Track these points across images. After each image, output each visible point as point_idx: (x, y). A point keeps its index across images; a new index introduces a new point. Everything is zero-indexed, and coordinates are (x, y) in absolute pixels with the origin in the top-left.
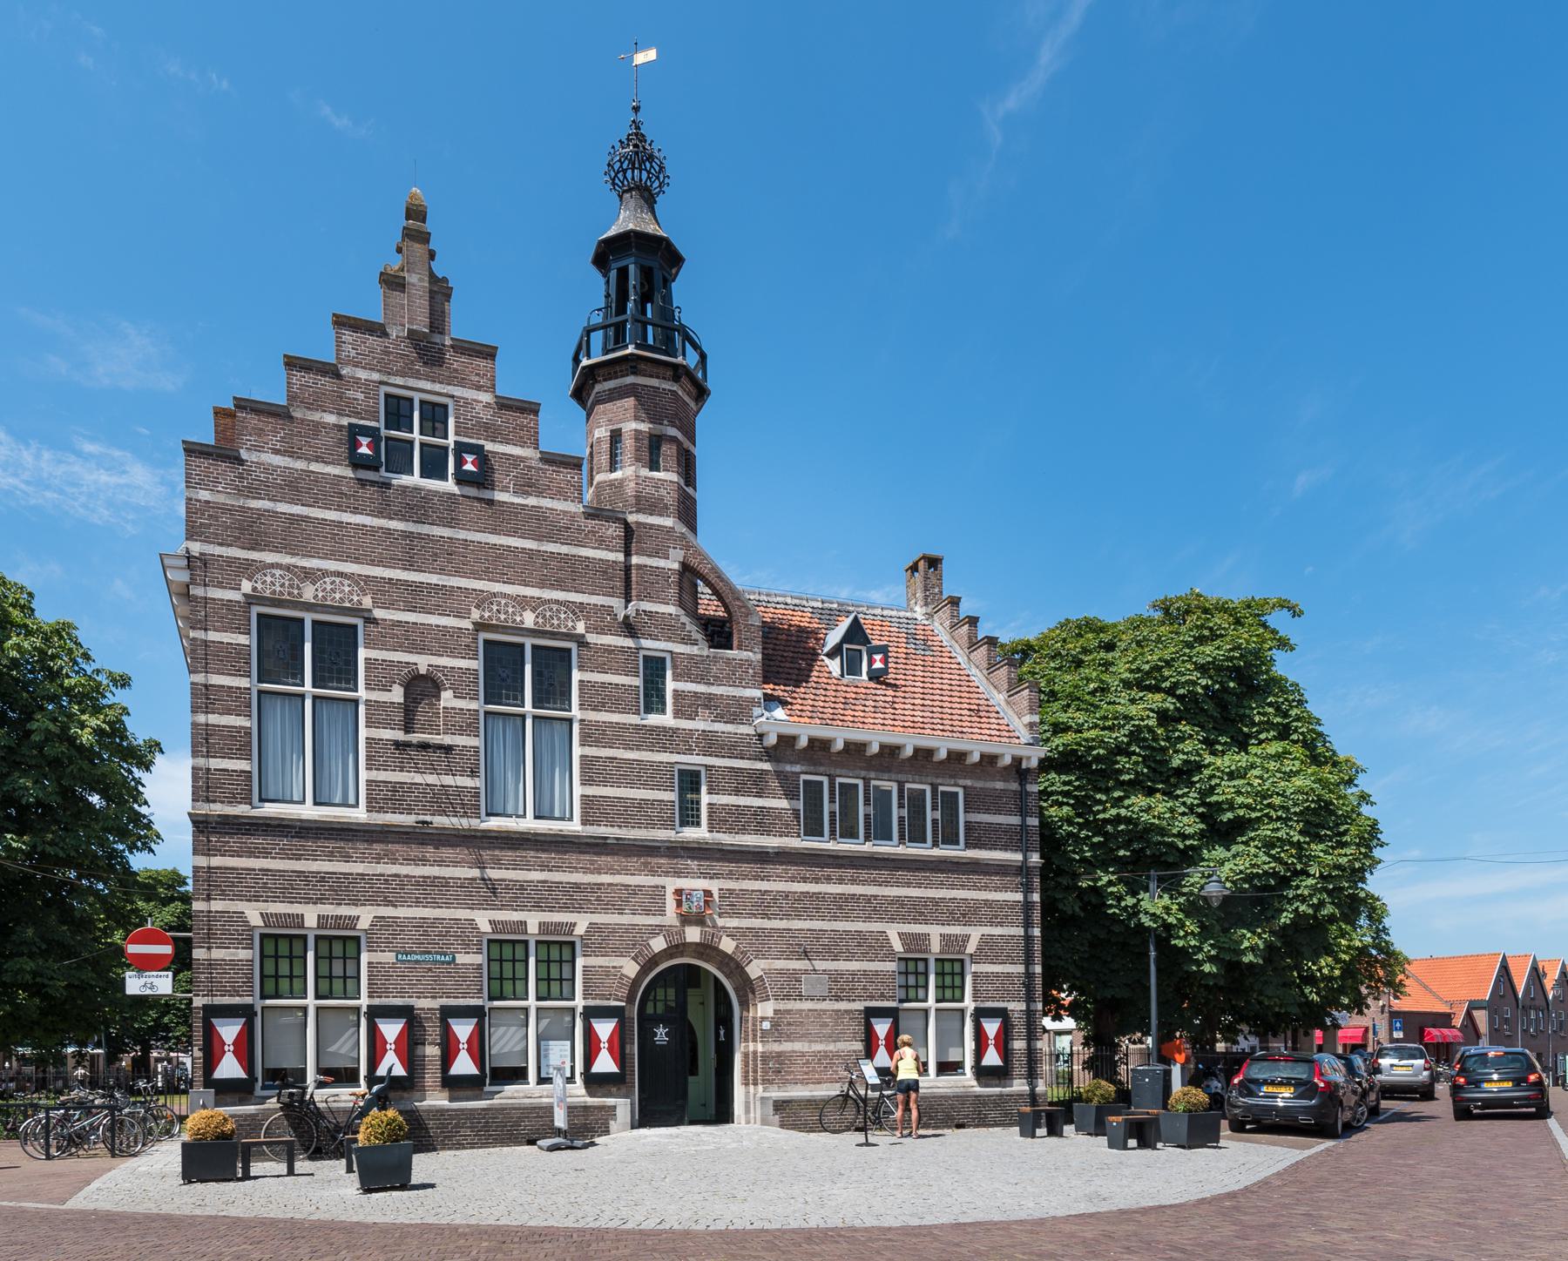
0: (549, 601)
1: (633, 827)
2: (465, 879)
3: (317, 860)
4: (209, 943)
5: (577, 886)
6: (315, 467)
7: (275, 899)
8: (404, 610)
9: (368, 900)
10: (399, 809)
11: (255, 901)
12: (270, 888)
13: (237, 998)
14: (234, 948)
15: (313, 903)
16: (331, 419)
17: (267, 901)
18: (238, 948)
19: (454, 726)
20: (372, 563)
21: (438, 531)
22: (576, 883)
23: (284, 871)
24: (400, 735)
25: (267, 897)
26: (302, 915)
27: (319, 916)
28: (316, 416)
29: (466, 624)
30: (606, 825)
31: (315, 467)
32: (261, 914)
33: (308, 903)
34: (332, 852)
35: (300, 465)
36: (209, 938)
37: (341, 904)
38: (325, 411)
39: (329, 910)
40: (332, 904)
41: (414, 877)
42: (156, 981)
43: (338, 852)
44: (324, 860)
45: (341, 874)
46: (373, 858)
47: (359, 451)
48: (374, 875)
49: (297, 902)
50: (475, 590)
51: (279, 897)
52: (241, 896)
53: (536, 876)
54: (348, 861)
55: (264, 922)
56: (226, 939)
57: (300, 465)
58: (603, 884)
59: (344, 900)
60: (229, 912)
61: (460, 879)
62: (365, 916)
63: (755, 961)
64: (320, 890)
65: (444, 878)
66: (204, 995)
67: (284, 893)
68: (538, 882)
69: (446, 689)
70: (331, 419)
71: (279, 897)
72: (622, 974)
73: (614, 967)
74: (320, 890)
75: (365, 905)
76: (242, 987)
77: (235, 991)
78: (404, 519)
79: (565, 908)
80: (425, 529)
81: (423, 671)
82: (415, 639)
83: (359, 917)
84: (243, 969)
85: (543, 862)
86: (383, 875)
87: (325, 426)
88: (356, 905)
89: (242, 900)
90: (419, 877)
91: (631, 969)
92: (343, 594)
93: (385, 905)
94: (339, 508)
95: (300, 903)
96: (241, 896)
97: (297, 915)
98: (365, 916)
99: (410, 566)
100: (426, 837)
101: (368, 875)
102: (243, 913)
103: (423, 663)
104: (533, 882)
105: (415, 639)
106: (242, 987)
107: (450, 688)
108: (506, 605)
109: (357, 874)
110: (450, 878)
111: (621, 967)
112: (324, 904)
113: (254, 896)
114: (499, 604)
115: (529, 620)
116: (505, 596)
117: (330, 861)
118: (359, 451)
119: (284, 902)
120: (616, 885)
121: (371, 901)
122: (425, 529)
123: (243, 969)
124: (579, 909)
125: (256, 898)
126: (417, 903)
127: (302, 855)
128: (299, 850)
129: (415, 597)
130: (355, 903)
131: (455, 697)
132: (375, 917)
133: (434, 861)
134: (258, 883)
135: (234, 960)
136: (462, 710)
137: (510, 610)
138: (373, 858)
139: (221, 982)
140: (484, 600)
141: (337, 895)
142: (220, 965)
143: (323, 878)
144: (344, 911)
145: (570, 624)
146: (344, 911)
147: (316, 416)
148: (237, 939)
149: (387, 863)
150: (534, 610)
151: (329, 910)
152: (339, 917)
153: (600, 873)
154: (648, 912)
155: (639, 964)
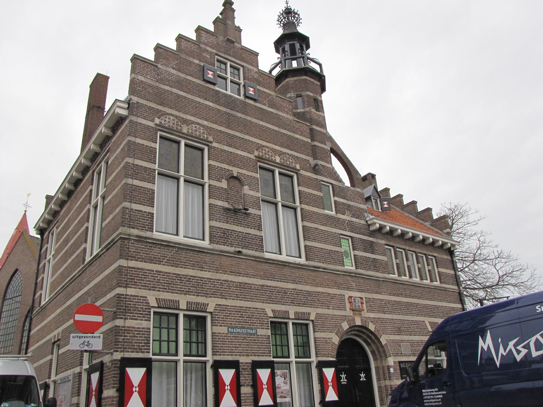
0: (285, 153)
1: (328, 264)
2: (259, 285)
3: (186, 268)
4: (125, 315)
5: (309, 293)
6: (189, 78)
7: (165, 290)
8: (226, 145)
9: (212, 294)
10: (227, 243)
11: (153, 290)
12: (161, 283)
13: (141, 354)
14: (141, 320)
15: (185, 294)
16: (197, 62)
17: (160, 291)
18: (142, 320)
19: (250, 203)
20: (213, 122)
21: (239, 115)
22: (308, 291)
23: (169, 273)
24: (226, 205)
25: (159, 288)
26: (179, 301)
27: (187, 302)
28: (191, 59)
29: (252, 156)
30: (318, 262)
31: (189, 78)
32: (156, 299)
33: (182, 294)
34: (194, 264)
35: (183, 75)
36: (126, 312)
37: (198, 296)
38: (194, 58)
39: (193, 299)
40: (194, 295)
41: (235, 282)
42: (91, 341)
43: (197, 265)
44: (190, 269)
45: (199, 277)
46: (214, 270)
47: (208, 76)
48: (215, 280)
49: (176, 293)
50: (255, 143)
51: (166, 289)
52: (145, 286)
53: (291, 286)
54: (202, 270)
55: (158, 304)
56: (136, 314)
57: (183, 75)
58: (319, 292)
59: (200, 293)
60: (138, 296)
61: (256, 285)
62: (212, 303)
63: (383, 335)
64: (188, 286)
65: (249, 284)
66: (121, 352)
67: (168, 286)
68: (292, 289)
69: (245, 185)
70: (197, 62)
71: (166, 289)
72: (333, 343)
73: (329, 338)
74: (188, 286)
75: (211, 297)
76: (144, 346)
77: (140, 349)
78: (225, 106)
79: (304, 304)
80: (234, 113)
81: (235, 175)
82: (232, 160)
83: (208, 304)
84: (144, 334)
85: (293, 278)
86: (220, 280)
87: (194, 63)
88: (206, 297)
89: (146, 289)
90: (238, 283)
91: (336, 340)
92: (200, 132)
93: (221, 298)
94: (199, 97)
95: (177, 293)
96: (145, 286)
97: (176, 301)
98: (212, 303)
99: (228, 127)
100: (240, 260)
101: (212, 279)
102: (146, 297)
103: (235, 171)
104: (289, 289)
105: (232, 160)
106: (144, 346)
107: (247, 185)
108: (268, 151)
109: (207, 278)
110: (252, 284)
111: (332, 338)
112: (190, 295)
113: (153, 287)
114: (265, 150)
115: (278, 160)
116: (268, 147)
117: (193, 269)
118: (208, 76)
119: (168, 292)
120: (325, 293)
121: (213, 295)
122: (234, 113)
123: (144, 334)
124: (311, 306)
125: (153, 289)
126: (237, 297)
127: (179, 264)
128: (177, 261)
129: (231, 141)
130: (206, 295)
131: (250, 189)
132: (216, 305)
133: (244, 274)
134: (155, 279)
135: (139, 328)
136: (253, 196)
137: (270, 154)
138: (214, 270)
139: (132, 343)
140: (259, 147)
141: (197, 290)
142: (132, 330)
143: (189, 278)
144: (201, 300)
145: (294, 165)
146: (201, 300)
147: (191, 59)
148: (142, 314)
149: (221, 273)
150: (279, 156)
151: (193, 299)
152: (198, 304)
153: (318, 286)
154: (339, 308)
155: (339, 337)
